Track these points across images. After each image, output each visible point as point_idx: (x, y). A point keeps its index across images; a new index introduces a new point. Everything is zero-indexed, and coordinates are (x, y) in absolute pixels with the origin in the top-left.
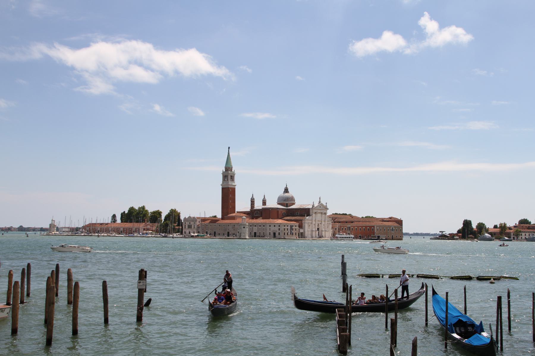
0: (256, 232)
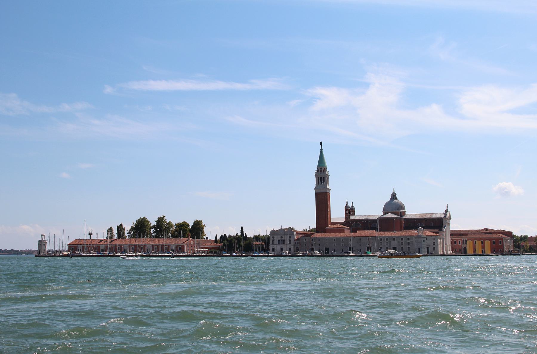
0: (396, 248)
